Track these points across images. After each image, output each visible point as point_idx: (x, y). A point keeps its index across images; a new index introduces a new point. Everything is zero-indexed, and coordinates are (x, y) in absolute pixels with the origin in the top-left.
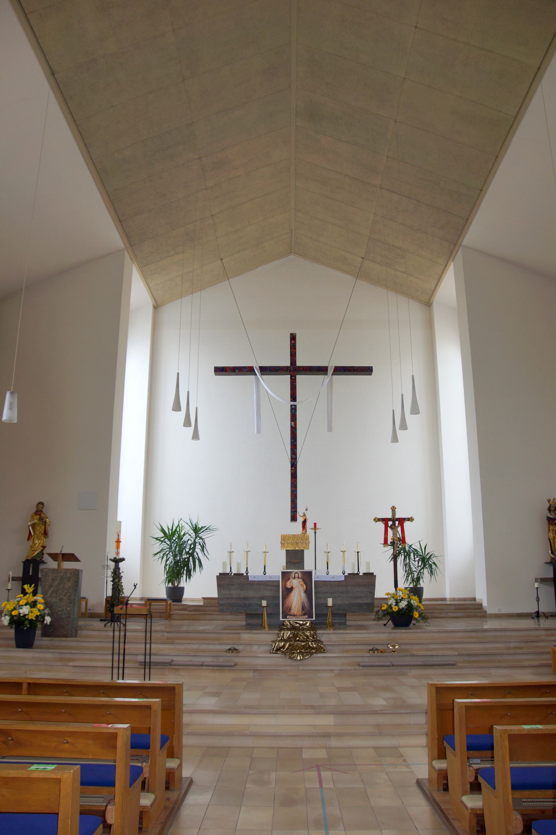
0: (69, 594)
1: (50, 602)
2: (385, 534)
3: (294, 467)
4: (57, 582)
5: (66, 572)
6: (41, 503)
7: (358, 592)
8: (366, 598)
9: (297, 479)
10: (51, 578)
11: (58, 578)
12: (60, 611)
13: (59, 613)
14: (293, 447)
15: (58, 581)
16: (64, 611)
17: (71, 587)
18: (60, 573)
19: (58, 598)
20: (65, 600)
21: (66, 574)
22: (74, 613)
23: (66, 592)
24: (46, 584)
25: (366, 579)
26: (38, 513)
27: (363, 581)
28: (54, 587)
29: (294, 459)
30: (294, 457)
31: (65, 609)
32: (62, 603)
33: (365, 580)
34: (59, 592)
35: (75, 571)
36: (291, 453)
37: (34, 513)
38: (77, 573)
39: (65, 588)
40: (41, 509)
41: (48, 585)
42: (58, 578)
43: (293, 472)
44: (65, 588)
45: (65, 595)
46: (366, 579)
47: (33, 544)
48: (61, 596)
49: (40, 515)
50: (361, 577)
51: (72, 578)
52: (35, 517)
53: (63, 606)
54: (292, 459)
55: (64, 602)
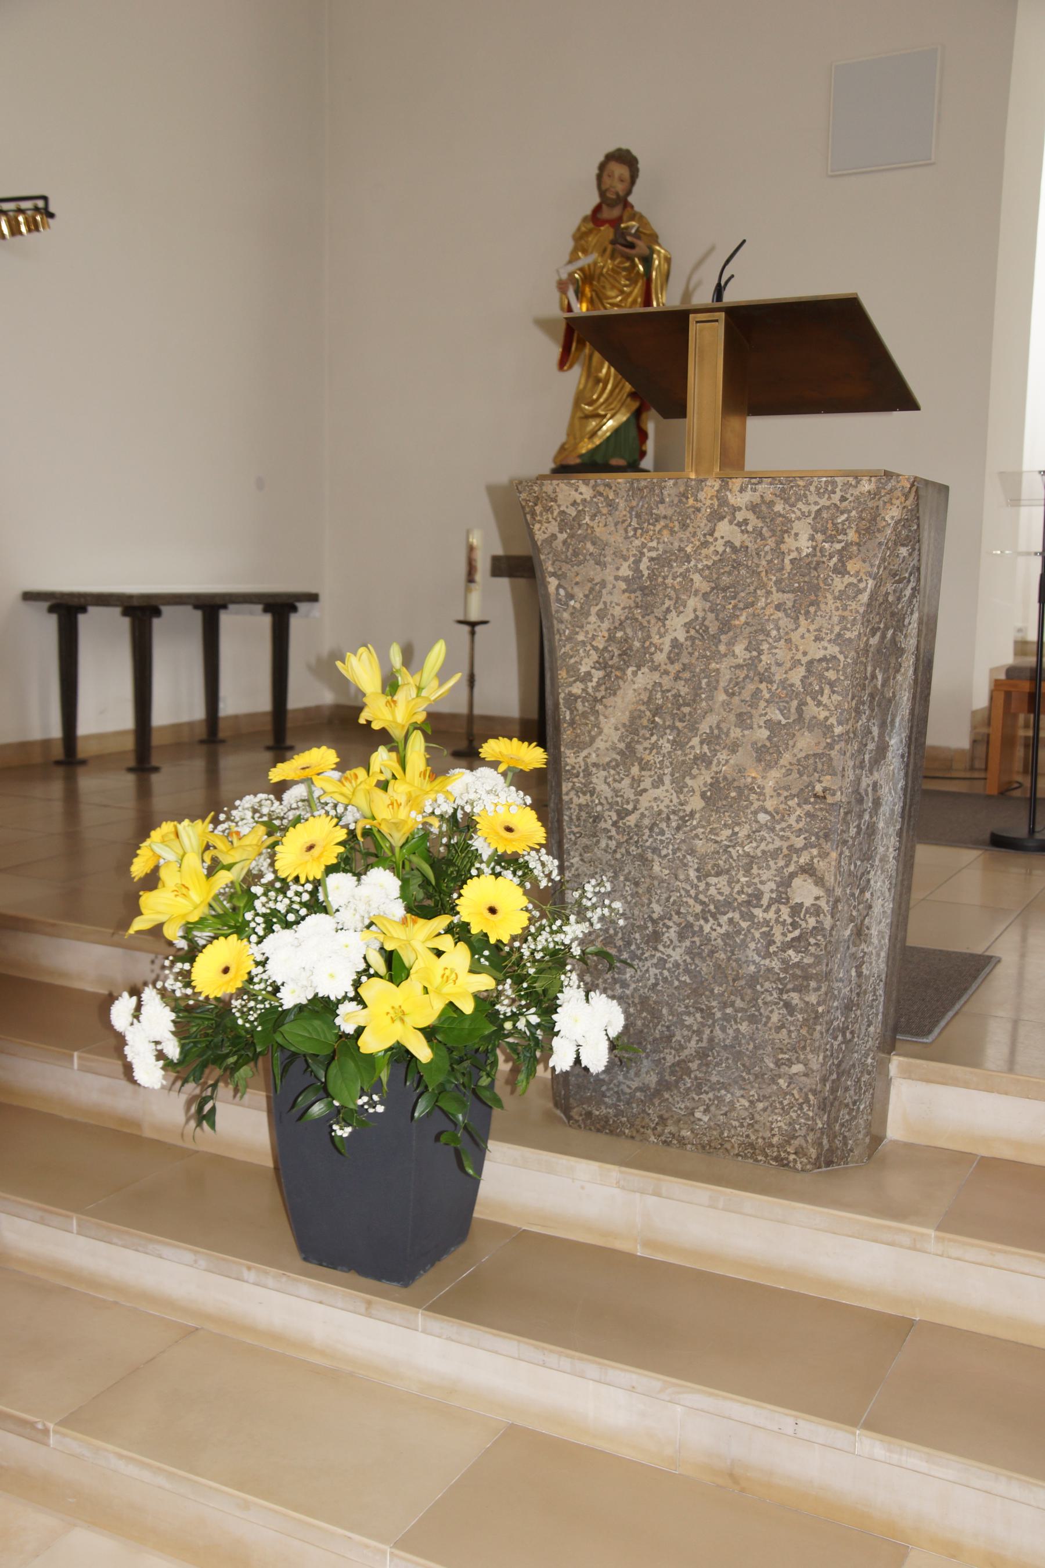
0: (806, 742)
1: (623, 814)
4: (688, 616)
5: (779, 507)
6: (624, 158)
10: (625, 571)
11: (696, 578)
12: (728, 904)
13: (714, 929)
15: (693, 602)
16: (758, 912)
17: (831, 675)
18: (716, 517)
19: (701, 780)
20: (769, 805)
21: (782, 529)
22: (860, 933)
23: (776, 716)
24: (581, 637)
26: (607, 214)
28: (655, 668)
31: (768, 889)
32: (743, 832)
34: (712, 720)
35: (874, 495)
37: (585, 220)
38: (893, 513)
39: (765, 678)
40: (620, 188)
41: (600, 643)
42: (696, 578)
44: (765, 678)
45: (765, 755)
47: (590, 384)
48: (725, 762)
49: (615, 223)
51: (841, 570)
52: (592, 240)
53: (751, 860)
55: (763, 817)
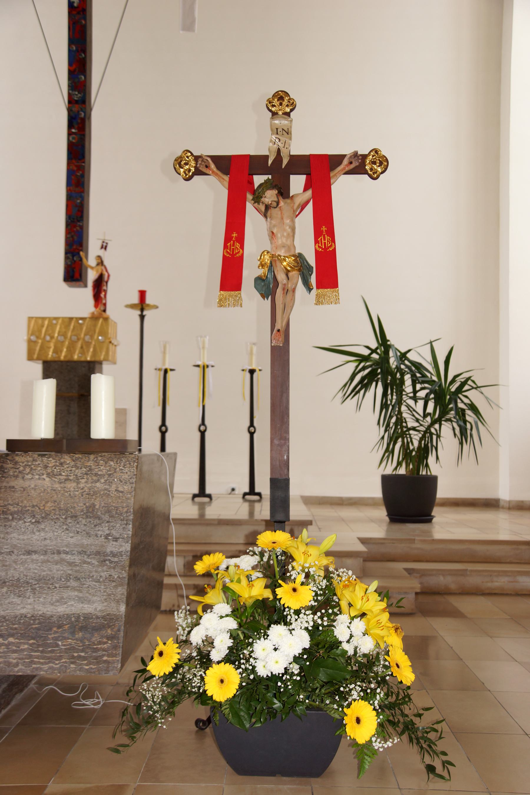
2: (228, 239)
3: (76, 126)
7: (29, 553)
8: (74, 589)
9: (84, 162)
14: (74, 67)
25: (77, 480)
27: (57, 486)
29: (77, 102)
30: (77, 96)
33: (71, 486)
36: (69, 86)
43: (74, 141)
46: (77, 480)
50: (46, 467)
54: (71, 101)
